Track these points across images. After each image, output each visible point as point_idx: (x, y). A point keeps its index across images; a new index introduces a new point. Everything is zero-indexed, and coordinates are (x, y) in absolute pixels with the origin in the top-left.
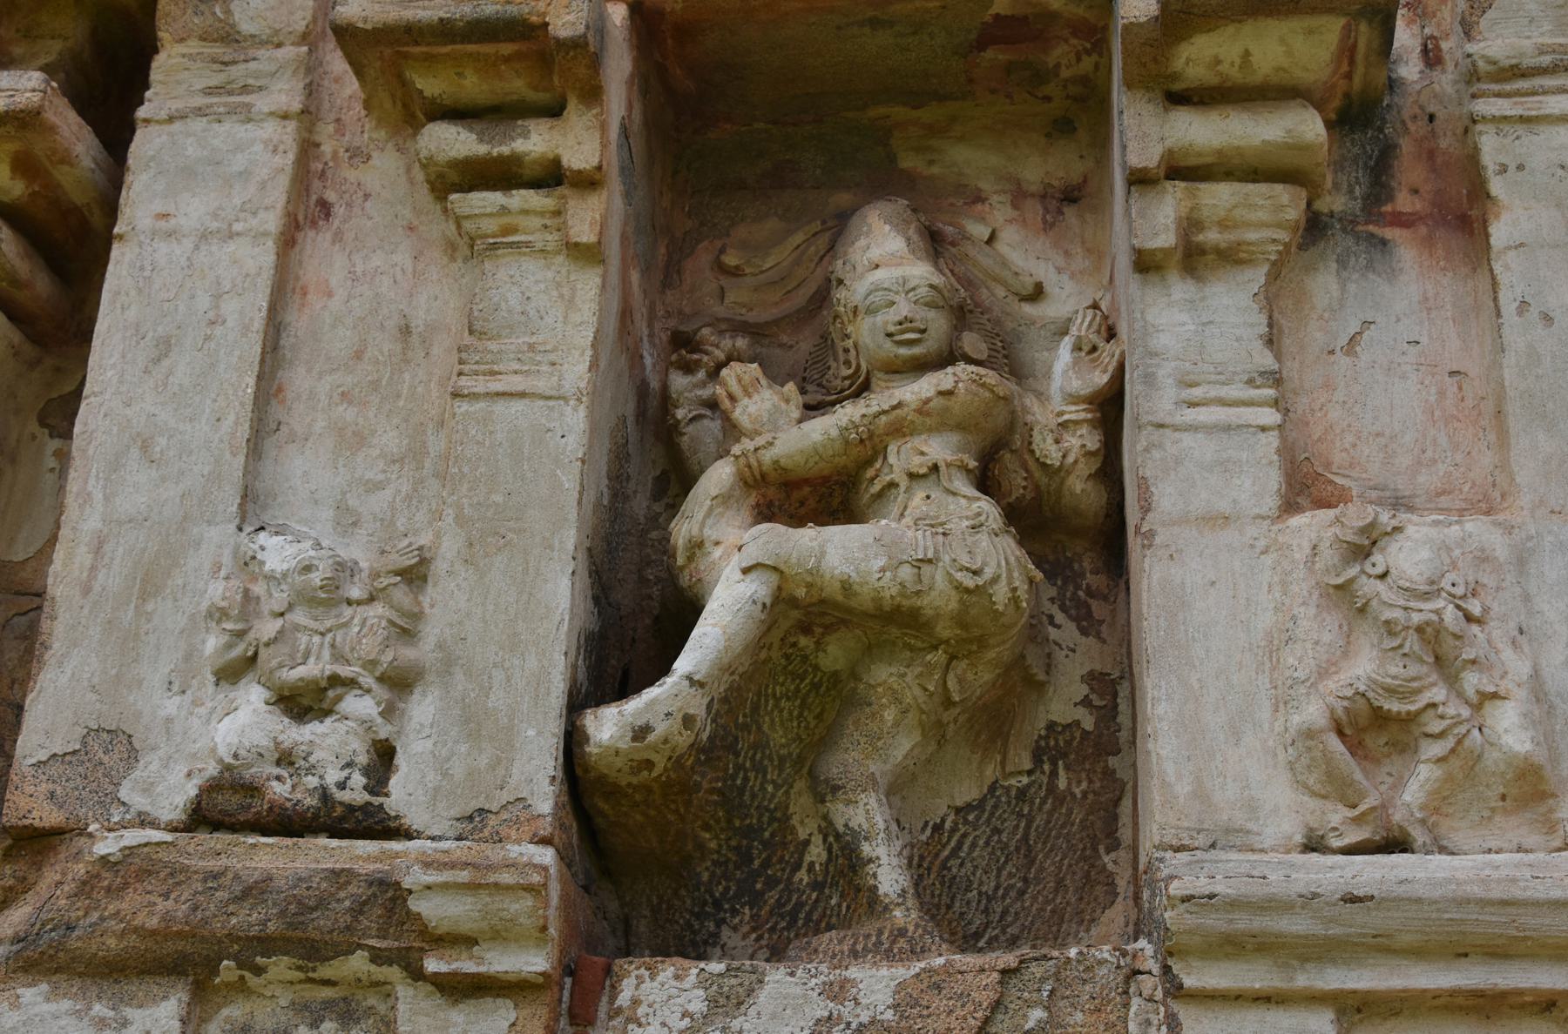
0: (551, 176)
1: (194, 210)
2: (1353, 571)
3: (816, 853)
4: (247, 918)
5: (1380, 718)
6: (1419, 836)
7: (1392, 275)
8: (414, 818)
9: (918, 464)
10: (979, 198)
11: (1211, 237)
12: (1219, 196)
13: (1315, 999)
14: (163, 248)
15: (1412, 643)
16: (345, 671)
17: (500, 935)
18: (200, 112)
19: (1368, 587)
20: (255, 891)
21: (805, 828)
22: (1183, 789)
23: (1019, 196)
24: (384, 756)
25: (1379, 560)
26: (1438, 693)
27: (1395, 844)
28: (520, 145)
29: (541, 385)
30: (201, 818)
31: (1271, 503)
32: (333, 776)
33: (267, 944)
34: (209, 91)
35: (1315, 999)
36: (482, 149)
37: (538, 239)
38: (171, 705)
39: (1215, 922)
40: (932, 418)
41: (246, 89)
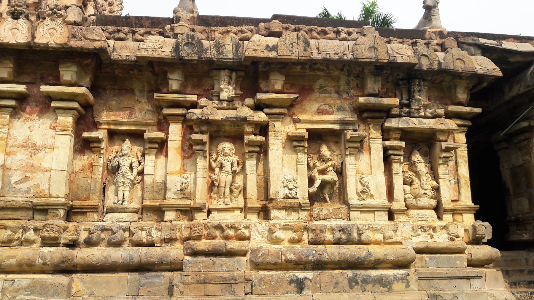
0: (303, 146)
1: (275, 147)
2: (361, 180)
3: (322, 197)
4: (289, 205)
5: (363, 191)
6: (365, 199)
7: (363, 155)
8: (299, 198)
9: (330, 170)
10: (330, 142)
11: (351, 153)
12: (352, 149)
13: (359, 211)
14: (273, 151)
15: (365, 186)
16: (293, 187)
17: (307, 207)
18: (274, 139)
19: (362, 182)
20: (290, 203)
21: (321, 195)
22: (350, 196)
23: (333, 142)
24: (296, 193)
25: (363, 180)
26: (367, 190)
27: (364, 200)
28: (301, 144)
29: (303, 164)
30: (284, 198)
31: (355, 174)
32: (294, 195)
33: (291, 207)
34: (274, 136)
35: (359, 211)
36: (298, 144)
37: (302, 151)
38: (281, 189)
39: (353, 206)
40: (331, 166)
41: (277, 136)
